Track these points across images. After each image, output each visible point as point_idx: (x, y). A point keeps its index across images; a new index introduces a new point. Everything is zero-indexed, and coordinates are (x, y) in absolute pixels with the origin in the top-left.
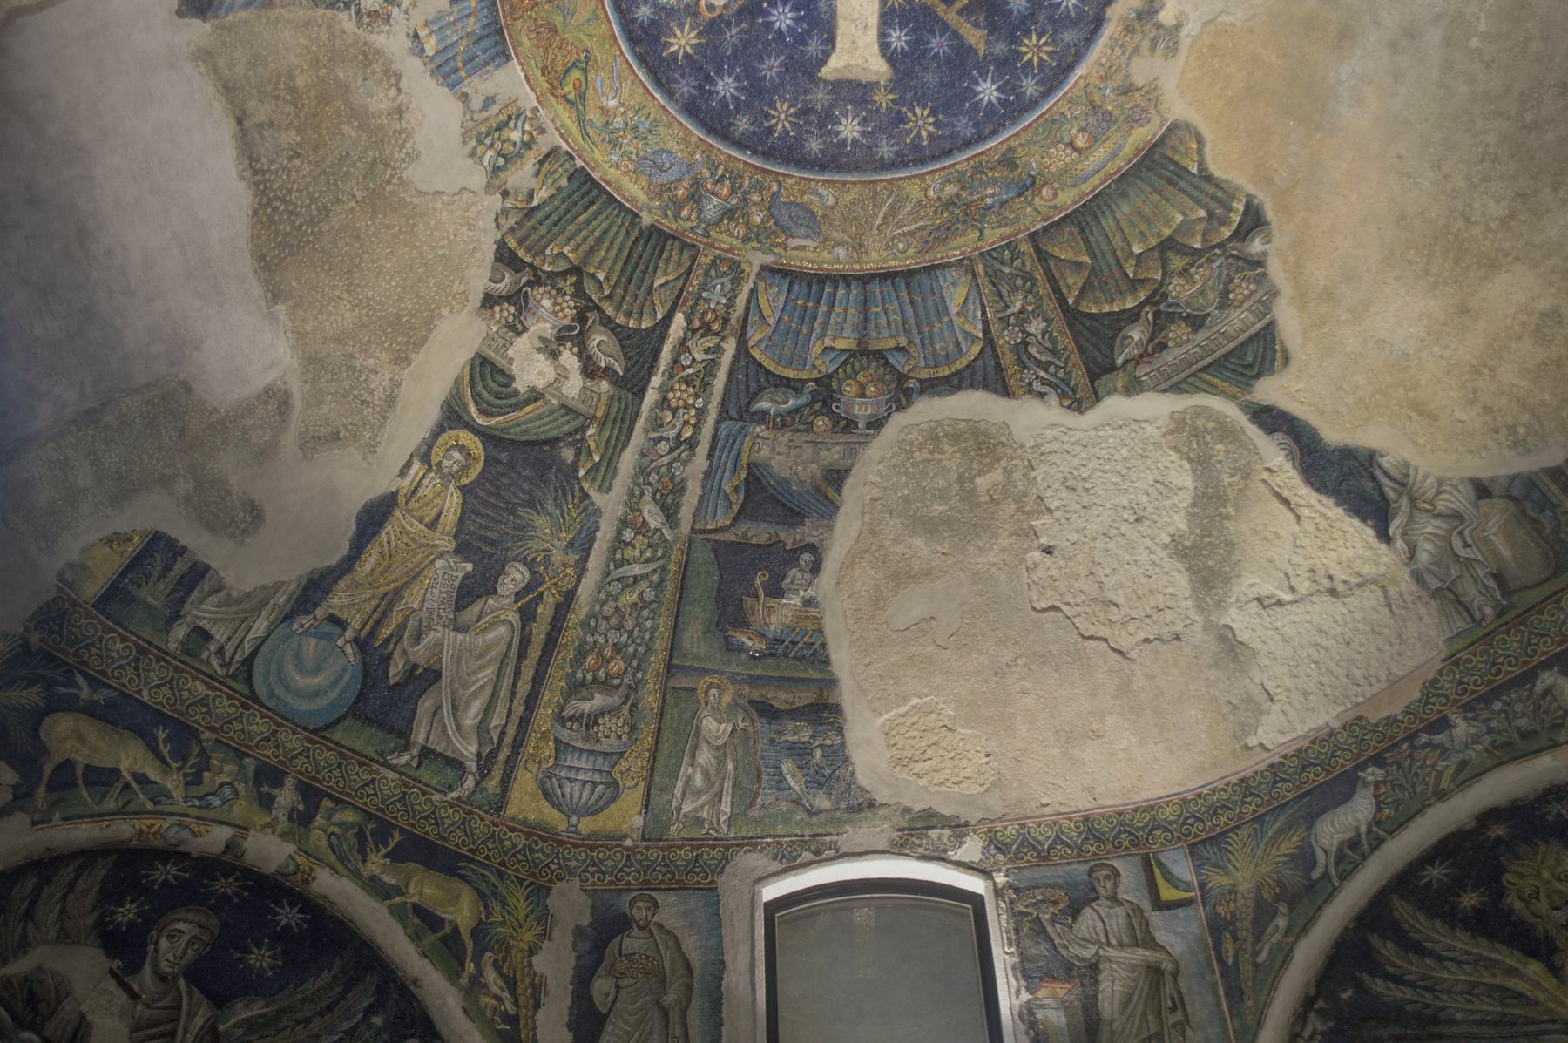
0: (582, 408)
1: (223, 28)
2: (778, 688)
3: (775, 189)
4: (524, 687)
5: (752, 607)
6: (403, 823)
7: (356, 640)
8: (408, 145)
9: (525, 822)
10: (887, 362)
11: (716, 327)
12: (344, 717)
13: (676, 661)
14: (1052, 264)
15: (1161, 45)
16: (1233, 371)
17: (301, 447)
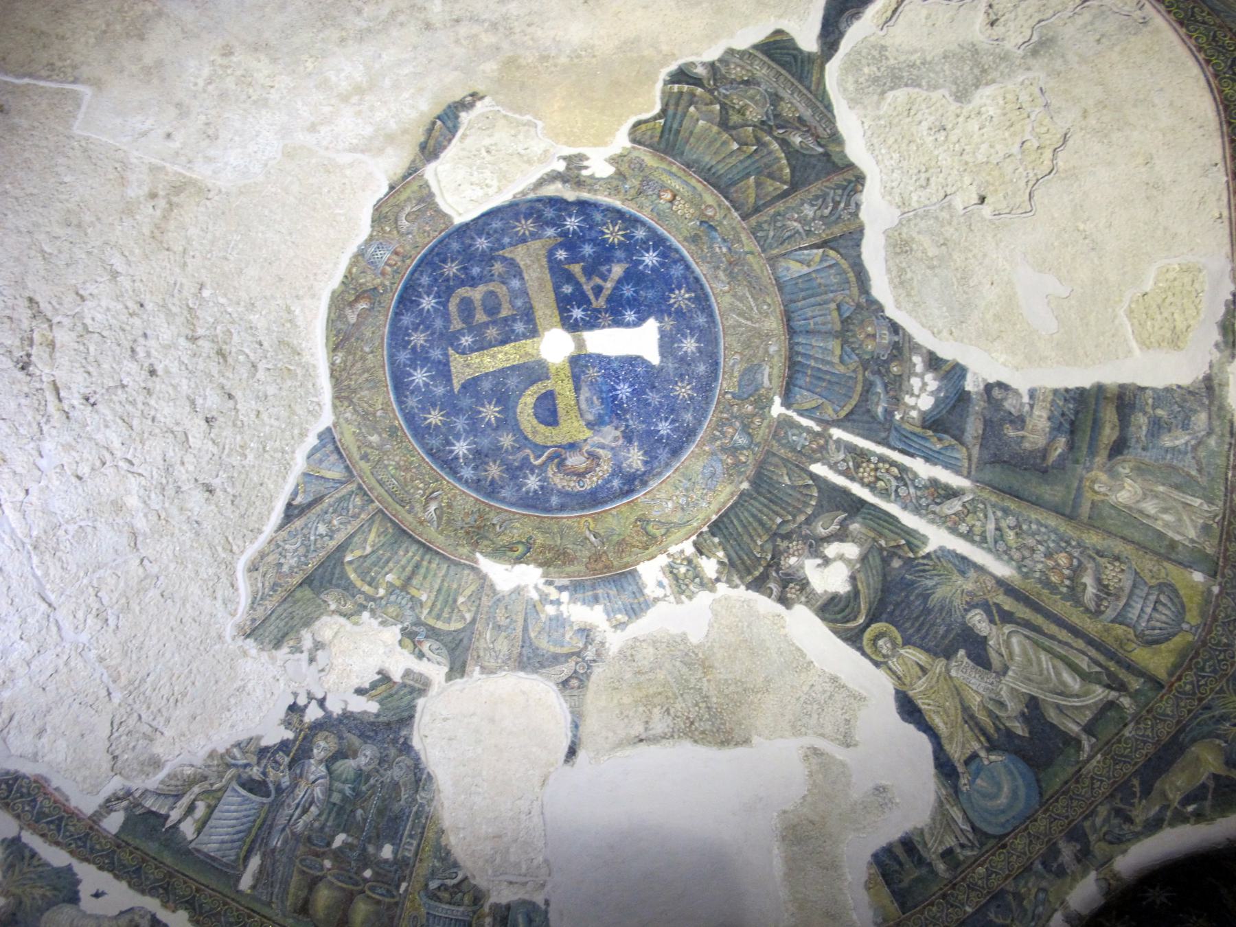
0: (867, 546)
2: (1100, 434)
3: (729, 396)
4: (1064, 635)
6: (1132, 769)
9: (1176, 666)
10: (849, 317)
11: (822, 442)
12: (1038, 781)
14: (762, 202)
16: (802, 71)
17: (848, 746)
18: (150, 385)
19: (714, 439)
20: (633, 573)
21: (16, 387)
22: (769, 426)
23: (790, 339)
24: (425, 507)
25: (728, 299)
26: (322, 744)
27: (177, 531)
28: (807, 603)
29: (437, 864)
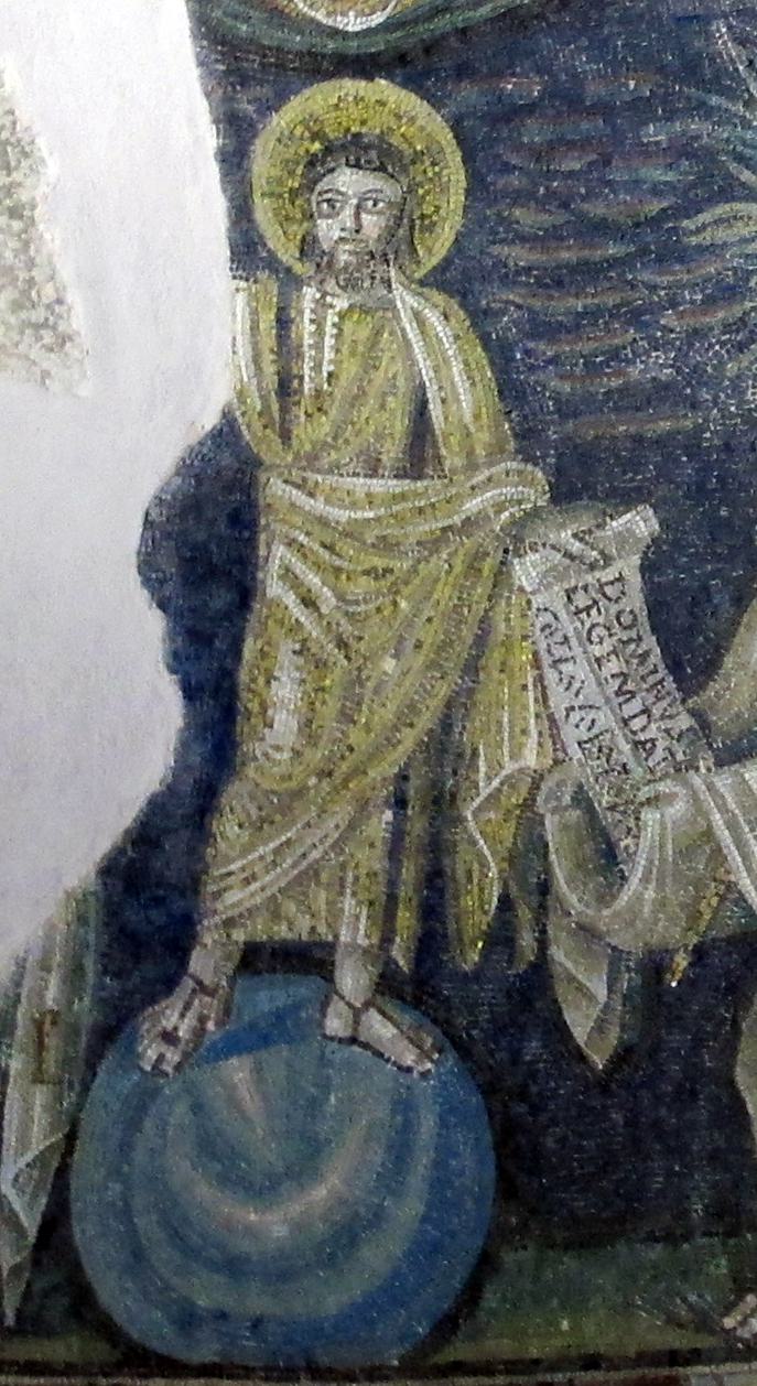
7: (388, 986)
12: (486, 1265)
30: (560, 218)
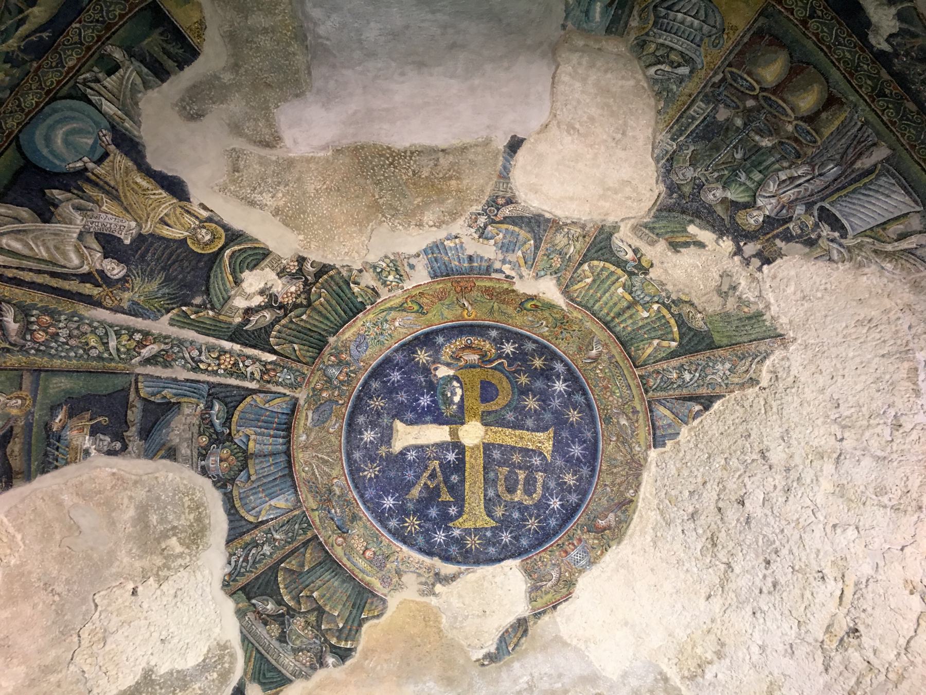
0: (227, 307)
1: (497, 154)
4: (28, 277)
5: (84, 418)
7: (86, 169)
8: (401, 227)
13: (43, 374)
14: (302, 550)
15: (424, 587)
17: (234, 149)
18: (774, 556)
19: (354, 372)
20: (434, 275)
21: (869, 621)
22: (309, 382)
23: (288, 449)
24: (600, 353)
25: (334, 473)
26: (752, 221)
27: (803, 444)
28: (280, 258)
29: (674, 87)
30: (180, 258)
